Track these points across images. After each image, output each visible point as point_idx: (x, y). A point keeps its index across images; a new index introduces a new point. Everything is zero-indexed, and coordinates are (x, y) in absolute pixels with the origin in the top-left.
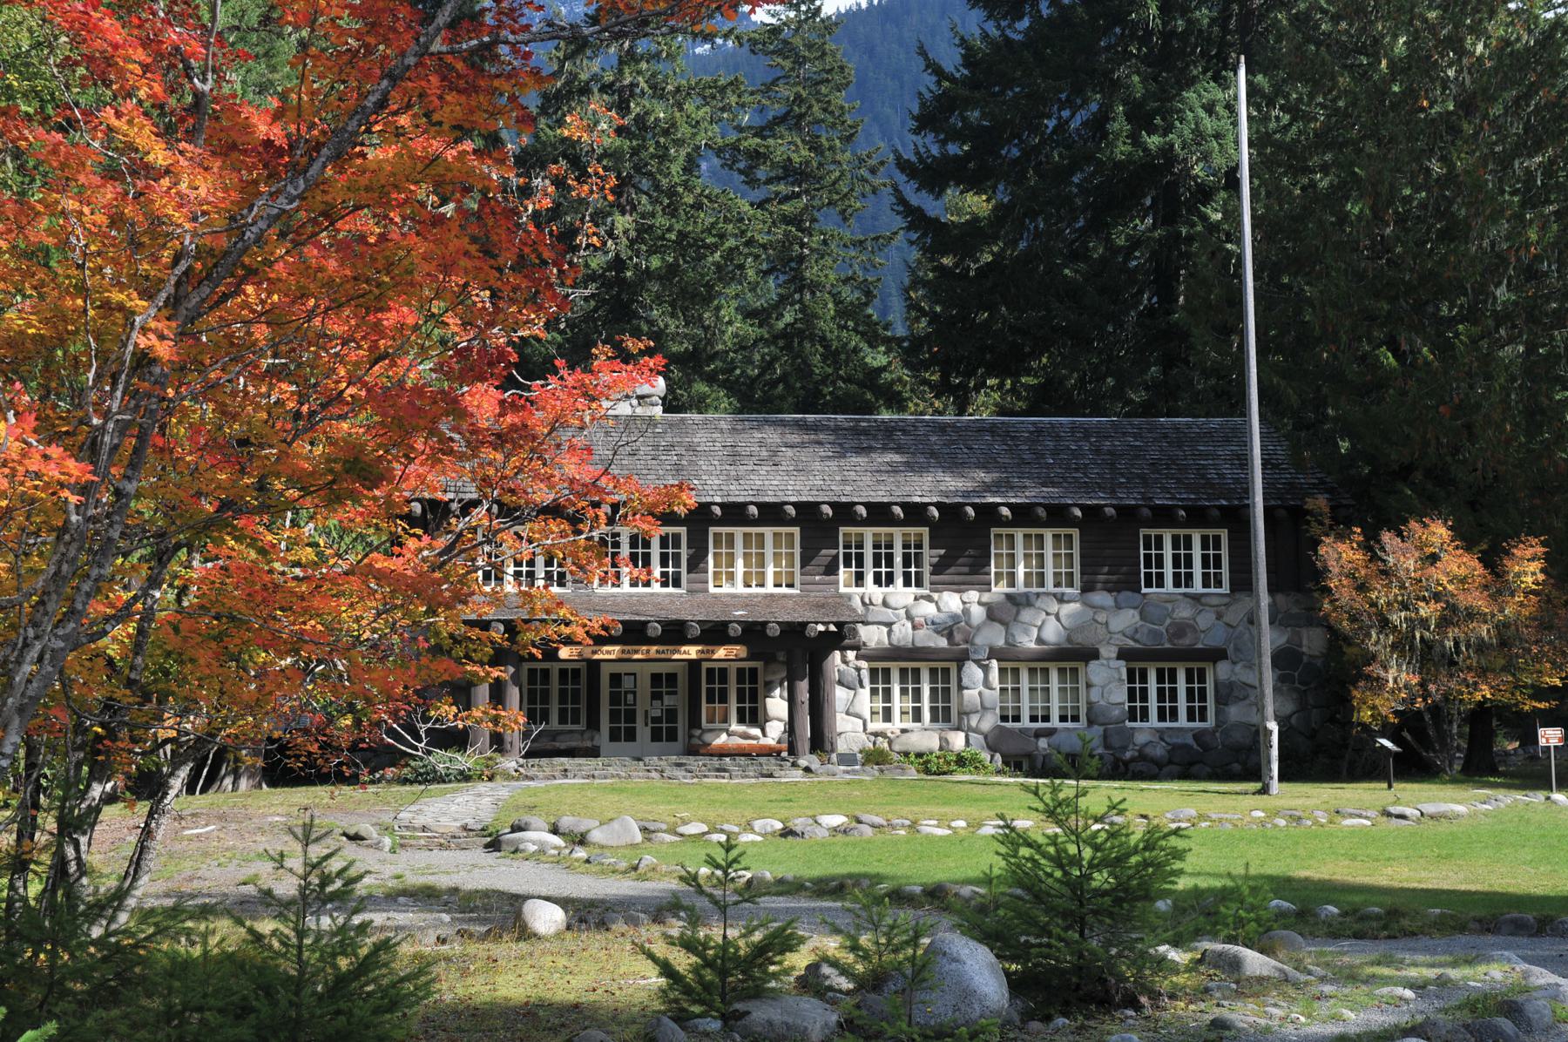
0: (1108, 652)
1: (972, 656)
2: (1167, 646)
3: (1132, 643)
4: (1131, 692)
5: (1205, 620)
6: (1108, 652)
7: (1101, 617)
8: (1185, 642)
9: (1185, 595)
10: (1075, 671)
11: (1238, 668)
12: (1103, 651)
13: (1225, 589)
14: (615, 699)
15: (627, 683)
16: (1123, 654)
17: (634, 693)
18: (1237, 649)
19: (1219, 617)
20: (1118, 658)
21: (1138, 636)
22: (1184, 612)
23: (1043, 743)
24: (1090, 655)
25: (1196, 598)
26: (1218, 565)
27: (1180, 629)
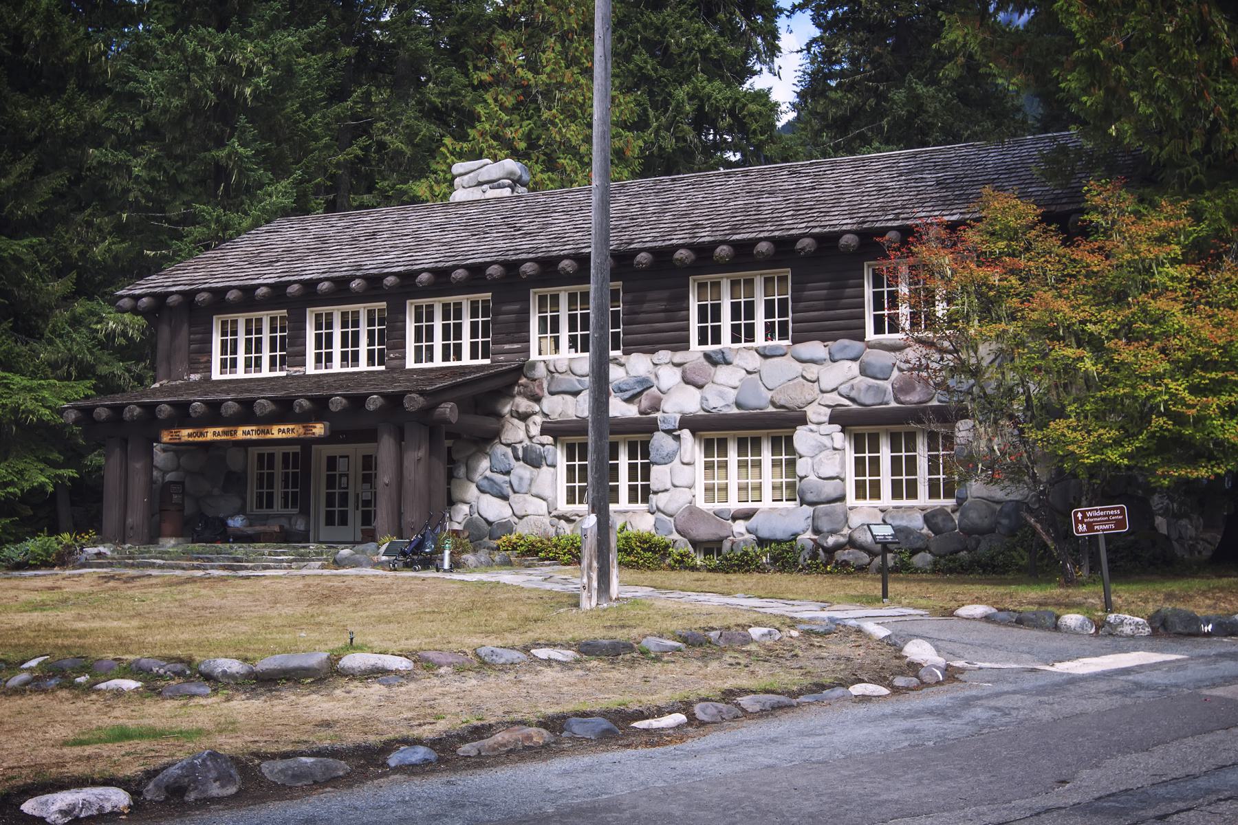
1: (661, 426)
2: (893, 404)
3: (847, 402)
4: (859, 462)
7: (812, 371)
10: (789, 440)
16: (839, 418)
17: (347, 475)
20: (832, 421)
21: (853, 394)
23: (740, 526)
24: (803, 420)
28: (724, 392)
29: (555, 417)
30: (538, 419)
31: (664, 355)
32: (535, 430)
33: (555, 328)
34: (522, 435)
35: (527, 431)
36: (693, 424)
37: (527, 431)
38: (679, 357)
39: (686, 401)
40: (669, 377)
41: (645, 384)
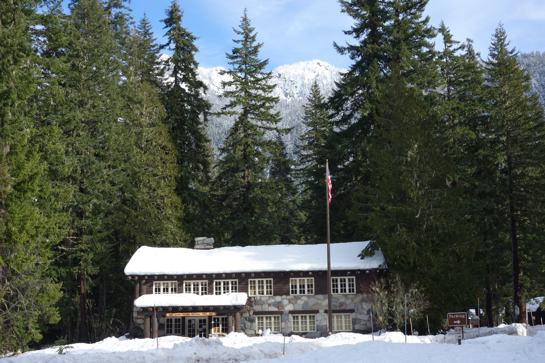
0: (322, 311)
5: (348, 302)
6: (322, 311)
7: (320, 302)
8: (343, 308)
9: (343, 295)
10: (314, 316)
11: (358, 315)
12: (320, 311)
13: (314, 294)
14: (190, 326)
15: (193, 322)
18: (357, 309)
19: (352, 300)
22: (342, 300)
24: (317, 312)
25: (346, 295)
26: (353, 286)
27: (341, 304)
28: (300, 305)
29: (257, 311)
30: (252, 311)
31: (284, 296)
32: (251, 313)
33: (255, 289)
34: (248, 315)
35: (249, 314)
36: (291, 312)
37: (249, 314)
38: (288, 297)
39: (289, 307)
40: (285, 302)
41: (280, 303)
